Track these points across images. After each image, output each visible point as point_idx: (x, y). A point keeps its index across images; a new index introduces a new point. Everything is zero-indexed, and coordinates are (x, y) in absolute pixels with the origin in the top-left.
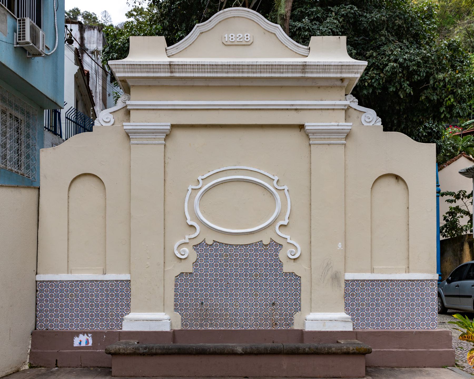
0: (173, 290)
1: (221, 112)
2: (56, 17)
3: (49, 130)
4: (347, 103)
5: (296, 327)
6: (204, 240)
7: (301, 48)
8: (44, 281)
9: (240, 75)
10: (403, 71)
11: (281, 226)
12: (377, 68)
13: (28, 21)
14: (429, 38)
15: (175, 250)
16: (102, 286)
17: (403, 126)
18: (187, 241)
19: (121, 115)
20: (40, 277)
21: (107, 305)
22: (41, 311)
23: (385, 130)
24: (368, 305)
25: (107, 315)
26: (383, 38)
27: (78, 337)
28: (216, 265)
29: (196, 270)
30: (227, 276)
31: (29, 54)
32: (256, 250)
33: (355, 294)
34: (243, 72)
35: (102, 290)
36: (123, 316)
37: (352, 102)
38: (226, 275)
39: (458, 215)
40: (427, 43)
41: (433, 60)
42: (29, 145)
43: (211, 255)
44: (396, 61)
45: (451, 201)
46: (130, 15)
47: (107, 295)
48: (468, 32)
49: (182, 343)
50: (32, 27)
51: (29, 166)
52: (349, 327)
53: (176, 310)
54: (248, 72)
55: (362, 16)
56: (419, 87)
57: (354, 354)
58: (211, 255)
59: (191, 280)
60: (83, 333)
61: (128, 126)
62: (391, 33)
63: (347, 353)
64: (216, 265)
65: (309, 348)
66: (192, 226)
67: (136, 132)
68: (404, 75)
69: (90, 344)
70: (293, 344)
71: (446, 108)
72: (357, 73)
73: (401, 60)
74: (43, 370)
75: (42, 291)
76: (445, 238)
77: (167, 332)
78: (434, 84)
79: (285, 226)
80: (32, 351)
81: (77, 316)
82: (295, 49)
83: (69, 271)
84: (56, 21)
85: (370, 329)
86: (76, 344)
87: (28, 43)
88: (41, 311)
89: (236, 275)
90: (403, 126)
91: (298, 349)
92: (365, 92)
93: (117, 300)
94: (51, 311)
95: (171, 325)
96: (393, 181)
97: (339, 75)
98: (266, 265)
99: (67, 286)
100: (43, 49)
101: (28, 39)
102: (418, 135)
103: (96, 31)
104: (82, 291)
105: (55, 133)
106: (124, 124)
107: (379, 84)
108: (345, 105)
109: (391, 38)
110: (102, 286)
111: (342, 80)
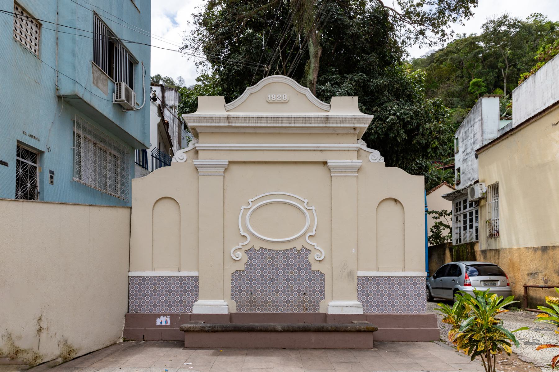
1: (265, 152)
3: (139, 165)
4: (359, 145)
5: (321, 311)
6: (253, 247)
7: (325, 105)
9: (280, 125)
10: (400, 122)
11: (310, 236)
12: (381, 119)
13: (123, 85)
14: (419, 98)
16: (177, 280)
17: (400, 162)
18: (240, 247)
19: (192, 154)
20: (131, 274)
21: (181, 295)
22: (132, 299)
23: (387, 165)
24: (374, 295)
25: (181, 302)
26: (385, 98)
28: (262, 265)
29: (247, 269)
31: (124, 109)
32: (292, 254)
33: (364, 286)
34: (281, 123)
35: (177, 284)
37: (363, 145)
38: (270, 273)
39: (442, 228)
40: (418, 101)
41: (422, 114)
42: (123, 175)
43: (258, 258)
44: (394, 114)
45: (436, 218)
46: (198, 80)
47: (181, 287)
48: (448, 93)
49: (237, 323)
50: (126, 89)
51: (123, 191)
52: (361, 312)
53: (232, 298)
54: (285, 123)
55: (369, 81)
56: (411, 133)
57: (364, 331)
58: (258, 258)
59: (244, 276)
60: (164, 315)
61: (197, 162)
62: (391, 94)
63: (359, 331)
64: (262, 265)
65: (331, 327)
66: (244, 236)
67: (203, 167)
68: (401, 125)
69: (169, 324)
70: (318, 324)
71: (432, 149)
72: (366, 123)
73: (398, 114)
74: (134, 343)
75: (133, 284)
76: (431, 245)
77: (225, 315)
78: (423, 131)
79: (313, 236)
81: (159, 302)
82: (320, 106)
83: (153, 269)
85: (376, 313)
86: (158, 323)
87: (123, 101)
88: (132, 299)
89: (277, 273)
90: (400, 162)
91: (323, 327)
92: (372, 137)
93: (188, 291)
94: (140, 299)
95: (229, 310)
96: (393, 203)
97: (352, 125)
98: (299, 265)
101: (123, 97)
102: (411, 169)
103: (173, 91)
104: (162, 284)
105: (143, 167)
106: (194, 160)
107: (382, 131)
108: (357, 148)
109: (391, 98)
110: (177, 280)
111: (355, 129)
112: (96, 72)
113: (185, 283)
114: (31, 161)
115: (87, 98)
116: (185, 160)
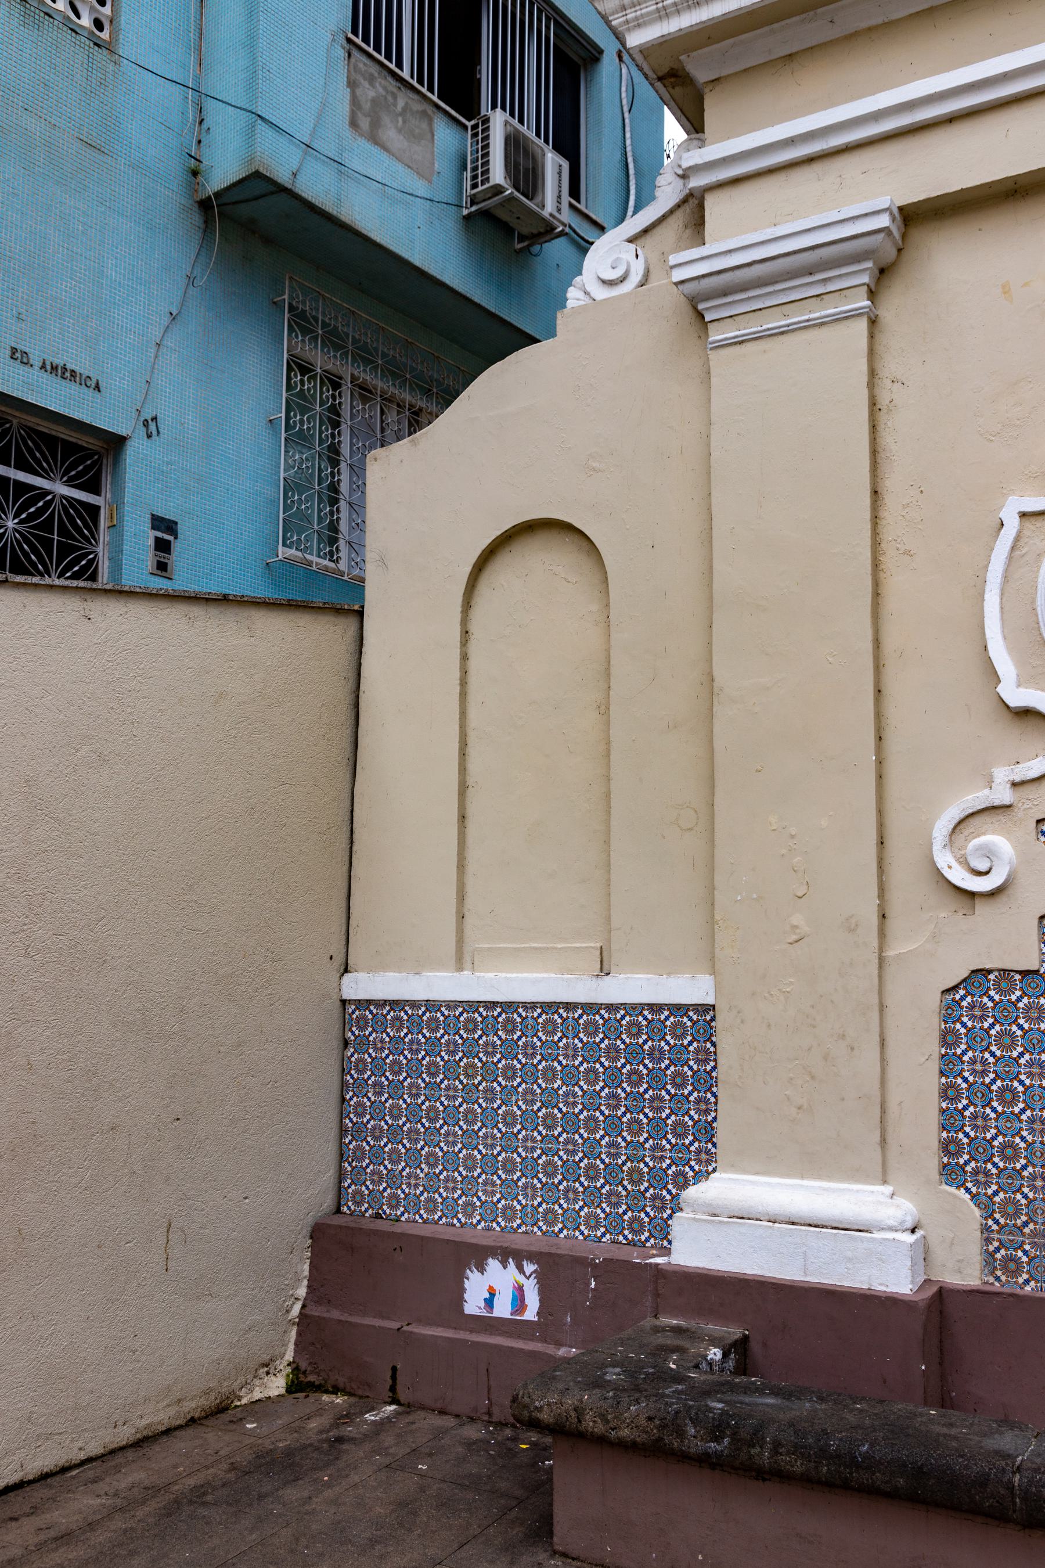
0: (934, 1066)
2: (628, 129)
8: (369, 1002)
15: (937, 847)
16: (591, 1029)
18: (1003, 795)
20: (360, 986)
27: (482, 1270)
35: (591, 1051)
36: (684, 1186)
60: (506, 1254)
61: (691, 263)
69: (531, 1314)
77: (891, 1302)
80: (307, 1311)
84: (628, 142)
86: (473, 1304)
94: (394, 1133)
99: (451, 1026)
100: (559, 210)
110: (591, 1029)
112: (371, 80)
113: (634, 1054)
114: (70, 483)
115: (317, 186)
116: (635, 278)
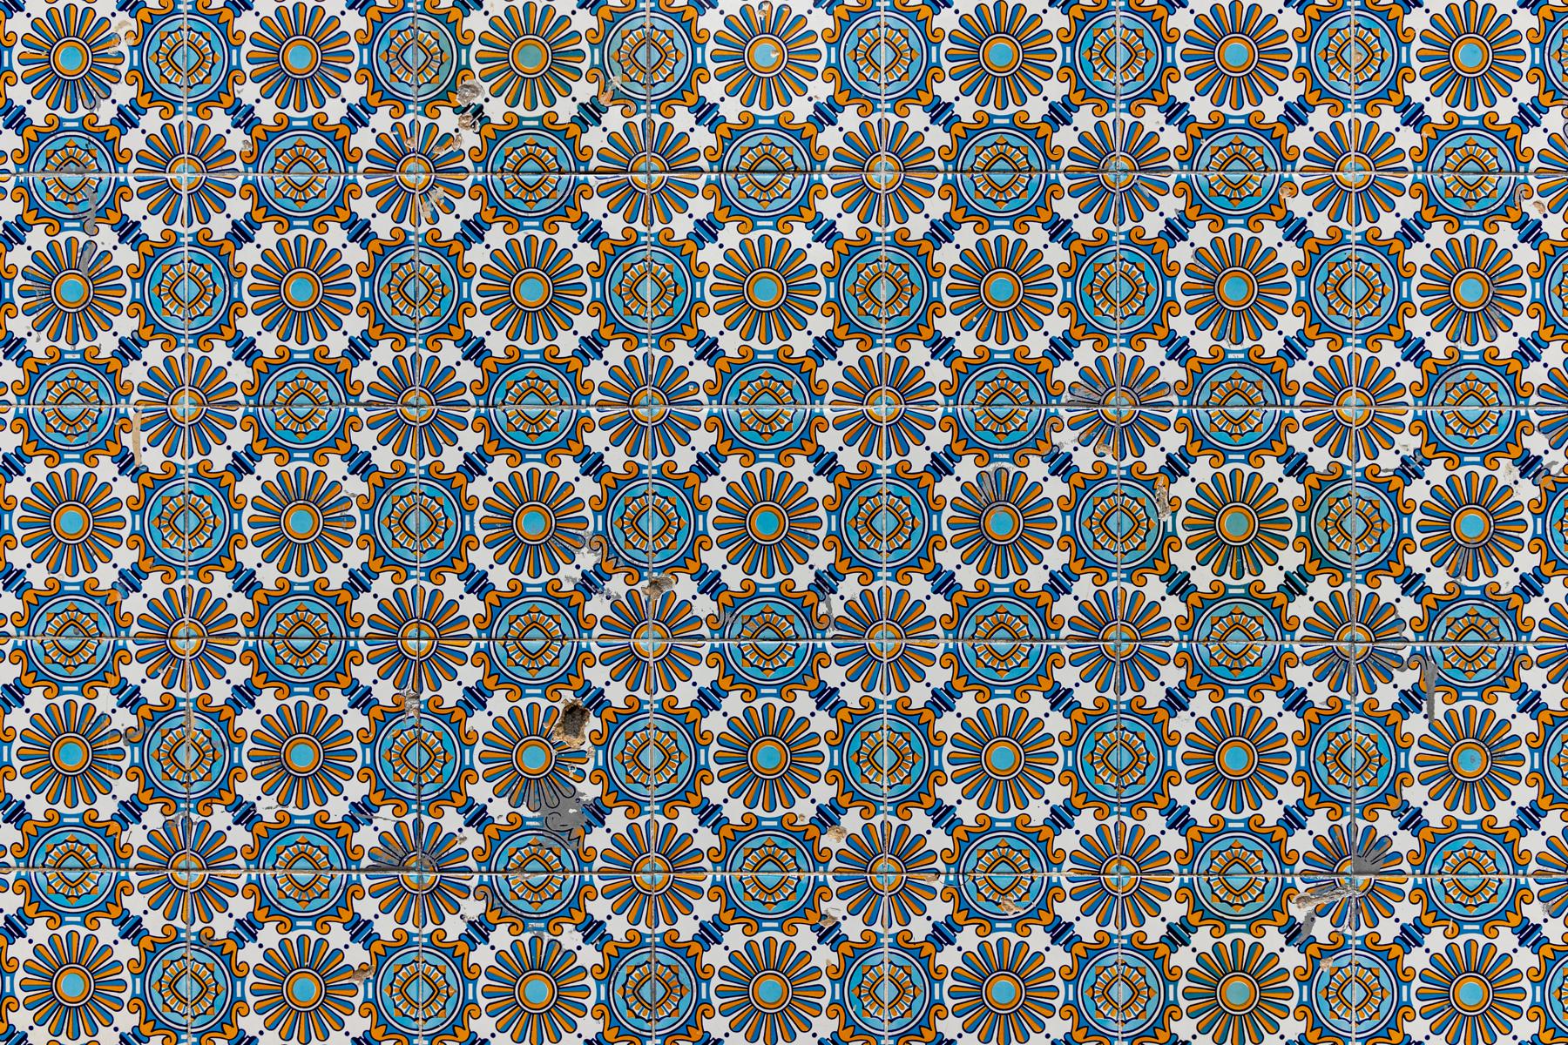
30: (559, 543)
